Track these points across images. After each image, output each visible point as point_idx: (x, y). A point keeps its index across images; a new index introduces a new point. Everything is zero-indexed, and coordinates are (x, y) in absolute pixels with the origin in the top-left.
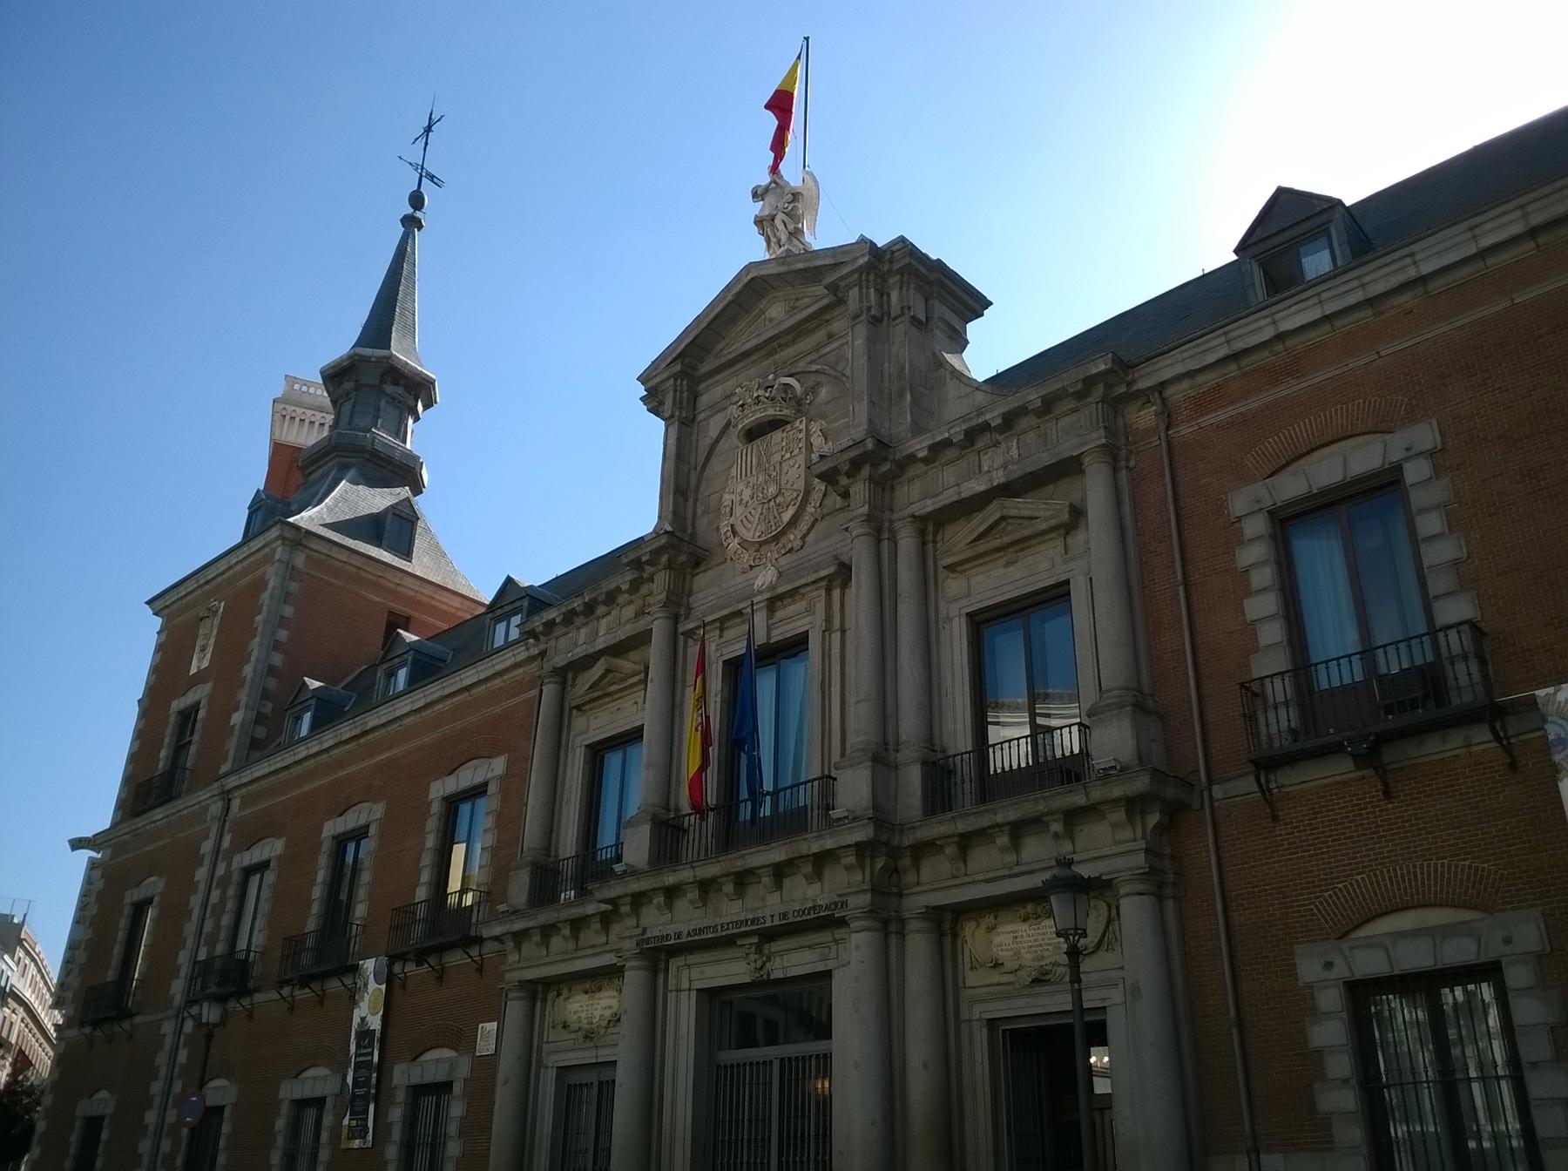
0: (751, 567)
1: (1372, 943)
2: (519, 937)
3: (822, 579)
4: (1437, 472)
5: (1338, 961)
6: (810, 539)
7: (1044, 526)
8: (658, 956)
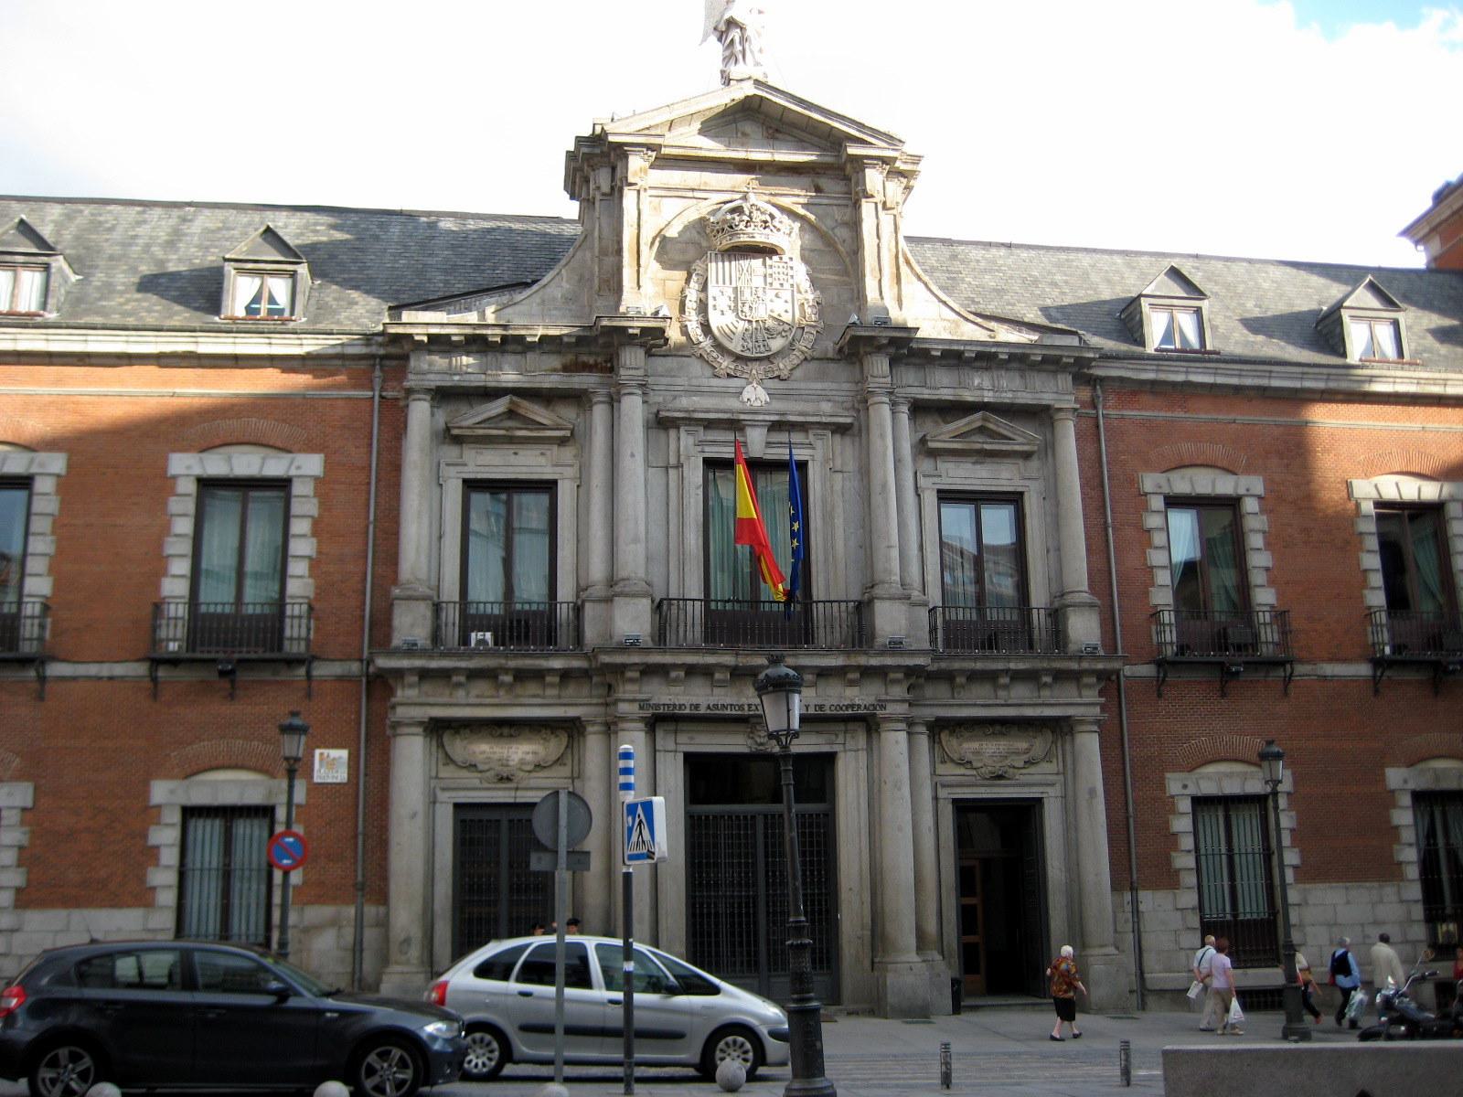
0: (729, 376)
1: (1209, 777)
2: (425, 675)
3: (834, 424)
4: (1263, 511)
5: (1189, 783)
6: (798, 373)
7: (1017, 448)
8: (658, 721)
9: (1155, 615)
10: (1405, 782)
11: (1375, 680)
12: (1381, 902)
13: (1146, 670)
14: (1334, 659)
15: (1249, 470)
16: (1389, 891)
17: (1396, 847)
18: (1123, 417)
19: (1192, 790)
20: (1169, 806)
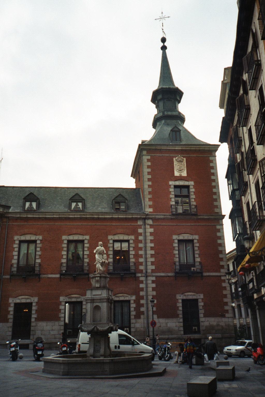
9: (12, 265)
10: (64, 300)
11: (60, 277)
12: (55, 326)
13: (8, 277)
14: (52, 274)
15: (39, 235)
16: (57, 323)
17: (60, 314)
18: (13, 225)
19: (14, 302)
20: (9, 305)
